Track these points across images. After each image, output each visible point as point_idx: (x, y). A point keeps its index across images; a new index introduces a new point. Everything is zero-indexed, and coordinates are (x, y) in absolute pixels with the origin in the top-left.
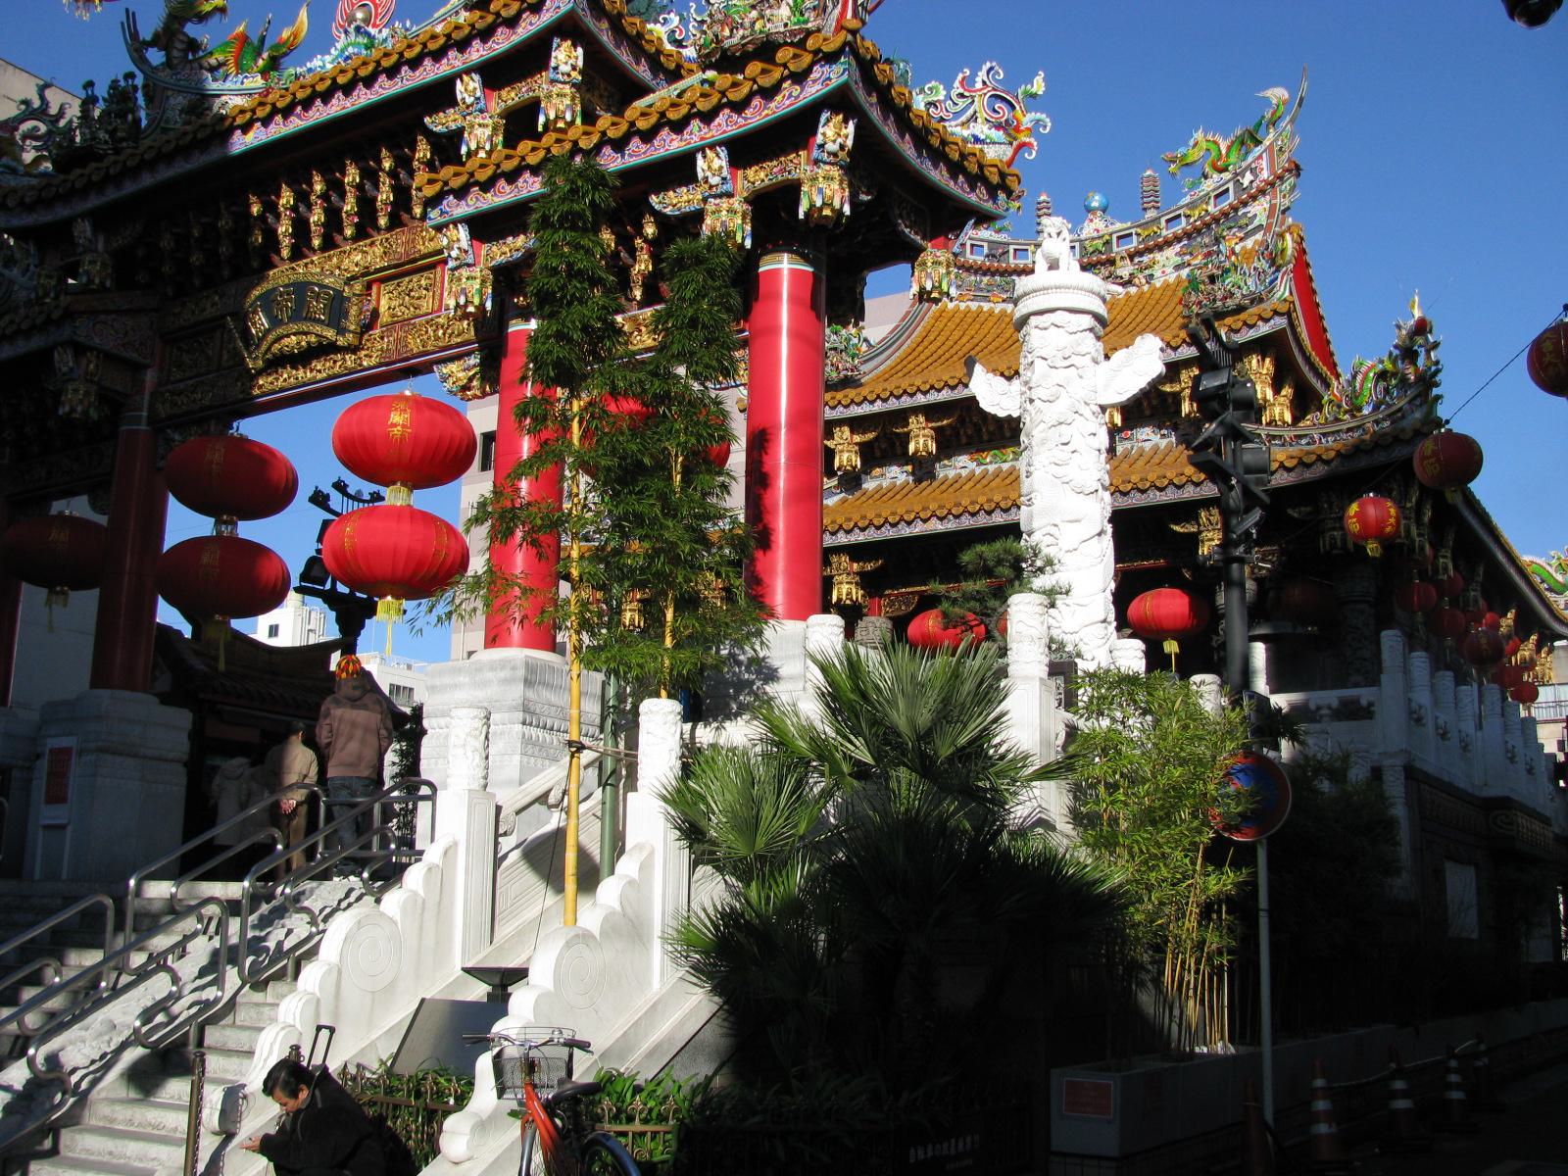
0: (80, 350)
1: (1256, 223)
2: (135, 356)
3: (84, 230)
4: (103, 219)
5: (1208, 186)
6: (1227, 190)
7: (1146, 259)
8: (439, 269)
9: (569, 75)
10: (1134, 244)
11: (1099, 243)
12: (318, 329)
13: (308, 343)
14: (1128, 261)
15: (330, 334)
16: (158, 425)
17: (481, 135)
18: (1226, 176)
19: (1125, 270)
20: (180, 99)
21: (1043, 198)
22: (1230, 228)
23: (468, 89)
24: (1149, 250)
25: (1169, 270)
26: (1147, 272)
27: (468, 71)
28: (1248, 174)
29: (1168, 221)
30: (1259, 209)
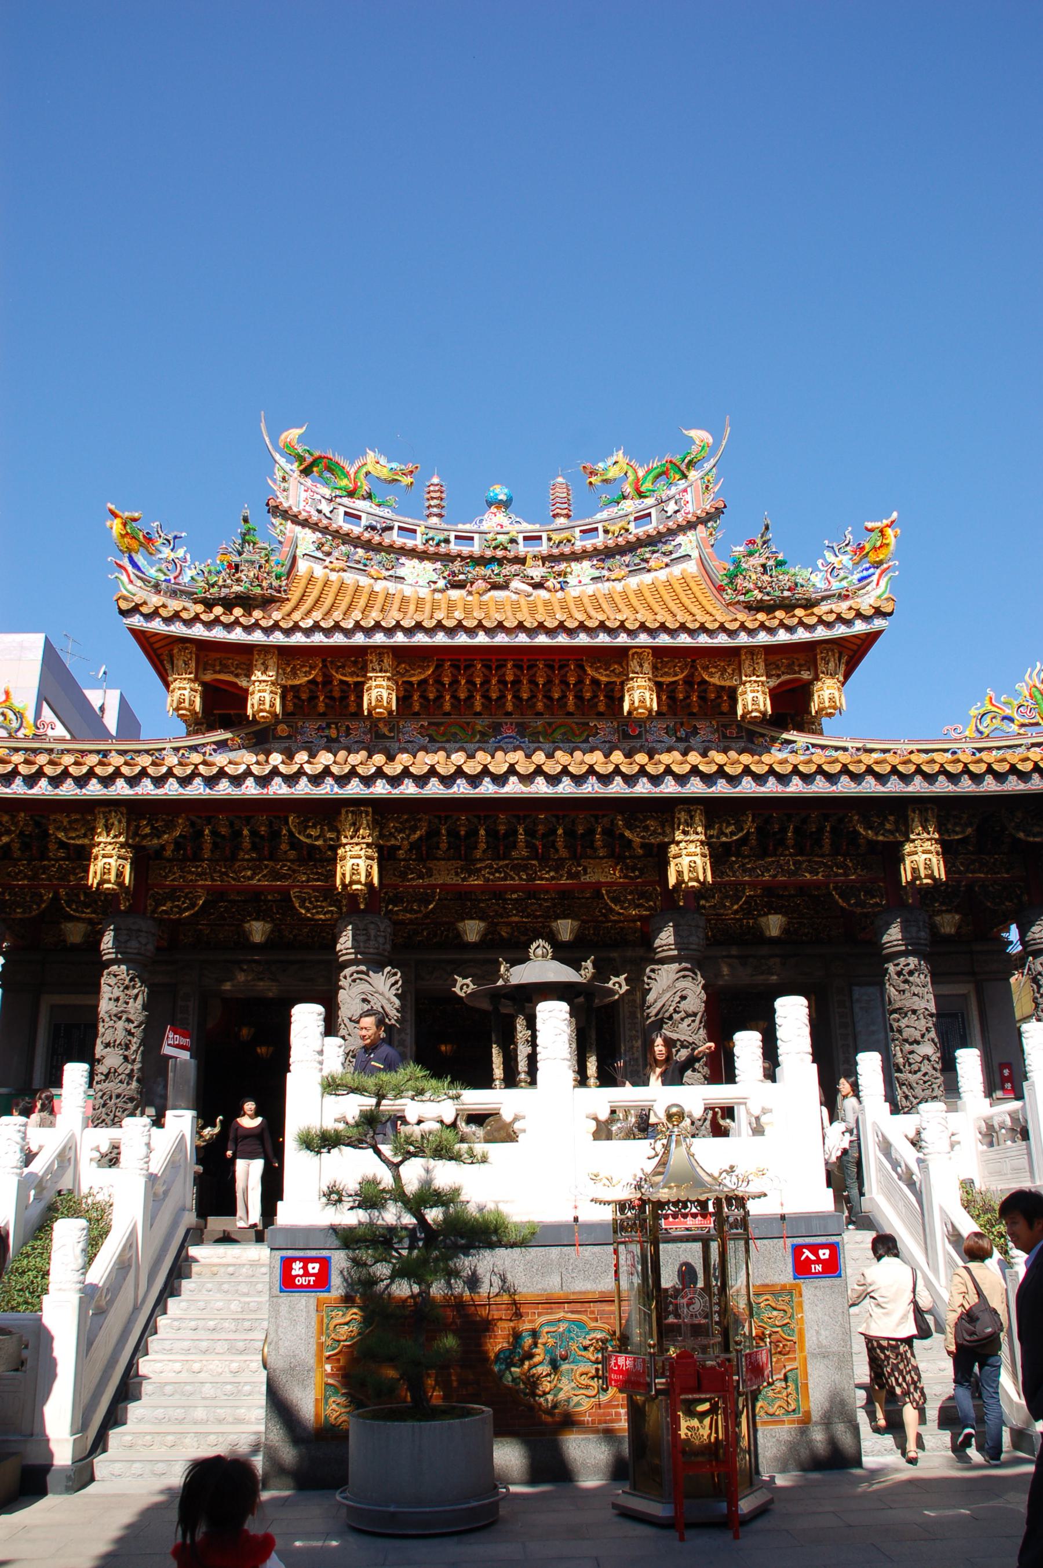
1: (681, 552)
5: (629, 506)
6: (649, 515)
7: (563, 566)
10: (544, 548)
11: (502, 538)
14: (540, 563)
18: (650, 501)
19: (537, 572)
21: (435, 480)
22: (654, 552)
24: (562, 558)
25: (586, 580)
26: (560, 579)
28: (673, 501)
29: (581, 531)
30: (687, 542)
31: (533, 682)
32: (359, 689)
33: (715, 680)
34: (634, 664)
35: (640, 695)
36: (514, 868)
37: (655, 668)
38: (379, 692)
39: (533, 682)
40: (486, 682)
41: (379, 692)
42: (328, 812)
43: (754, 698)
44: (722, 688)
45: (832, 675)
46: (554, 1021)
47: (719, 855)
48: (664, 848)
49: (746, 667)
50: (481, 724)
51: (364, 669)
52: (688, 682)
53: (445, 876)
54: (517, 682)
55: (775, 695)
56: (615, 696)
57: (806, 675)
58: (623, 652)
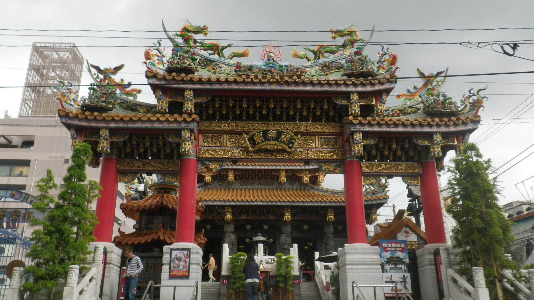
0: (191, 131)
3: (189, 94)
4: (197, 93)
12: (282, 144)
13: (277, 148)
15: (286, 147)
17: (356, 109)
23: (355, 97)
27: (356, 92)
31: (261, 174)
32: (227, 176)
33: (298, 175)
34: (281, 172)
35: (283, 179)
36: (257, 216)
37: (286, 172)
38: (231, 177)
39: (261, 174)
40: (252, 174)
41: (231, 177)
42: (223, 207)
43: (306, 179)
44: (300, 177)
45: (322, 175)
46: (261, 246)
47: (293, 215)
48: (283, 213)
49: (304, 173)
50: (251, 182)
51: (228, 172)
52: (293, 174)
53: (244, 217)
54: (258, 174)
55: (310, 178)
56: (278, 177)
57: (317, 174)
58: (279, 170)
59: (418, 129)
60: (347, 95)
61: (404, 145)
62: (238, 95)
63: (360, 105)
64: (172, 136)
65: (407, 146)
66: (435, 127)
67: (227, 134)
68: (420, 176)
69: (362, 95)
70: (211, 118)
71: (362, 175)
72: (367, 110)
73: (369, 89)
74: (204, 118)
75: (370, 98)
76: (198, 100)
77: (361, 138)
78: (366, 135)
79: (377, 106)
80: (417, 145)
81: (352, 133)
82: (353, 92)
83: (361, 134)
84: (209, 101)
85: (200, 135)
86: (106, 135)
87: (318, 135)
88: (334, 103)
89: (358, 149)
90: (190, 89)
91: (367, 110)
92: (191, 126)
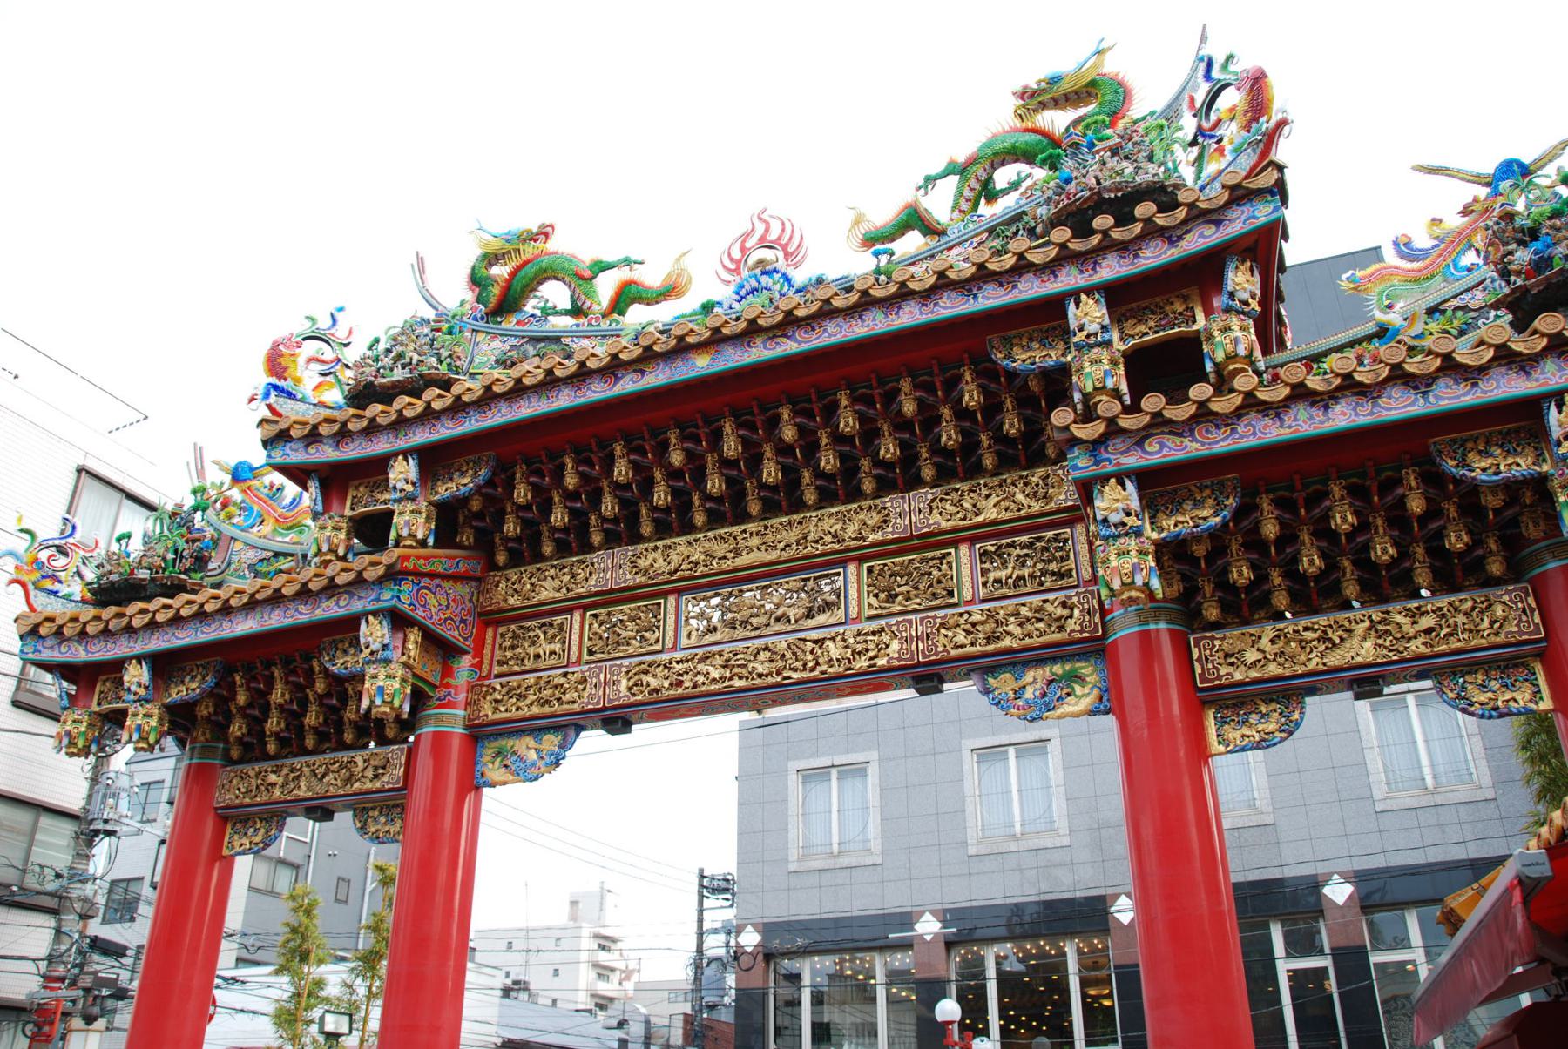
0: (399, 621)
2: (452, 634)
3: (403, 473)
4: (433, 461)
8: (964, 548)
9: (1246, 303)
16: (479, 734)
17: (1098, 372)
20: (497, 343)
23: (1089, 315)
27: (1089, 291)
59: (1450, 397)
60: (1047, 316)
61: (1401, 502)
62: (586, 432)
63: (1125, 354)
64: (345, 652)
65: (1416, 505)
66: (1549, 366)
67: (585, 608)
68: (1540, 655)
69: (1123, 299)
70: (526, 553)
71: (1206, 703)
72: (1166, 367)
73: (1155, 256)
74: (501, 558)
75: (1179, 307)
76: (444, 491)
77: (1135, 504)
78: (1159, 487)
79: (1210, 337)
80: (1474, 488)
81: (1087, 489)
82: (1075, 295)
83: (1130, 486)
84: (490, 483)
85: (490, 632)
86: (139, 684)
87: (972, 541)
88: (1012, 375)
89: (1130, 565)
90: (406, 453)
91: (1166, 367)
92: (387, 597)
